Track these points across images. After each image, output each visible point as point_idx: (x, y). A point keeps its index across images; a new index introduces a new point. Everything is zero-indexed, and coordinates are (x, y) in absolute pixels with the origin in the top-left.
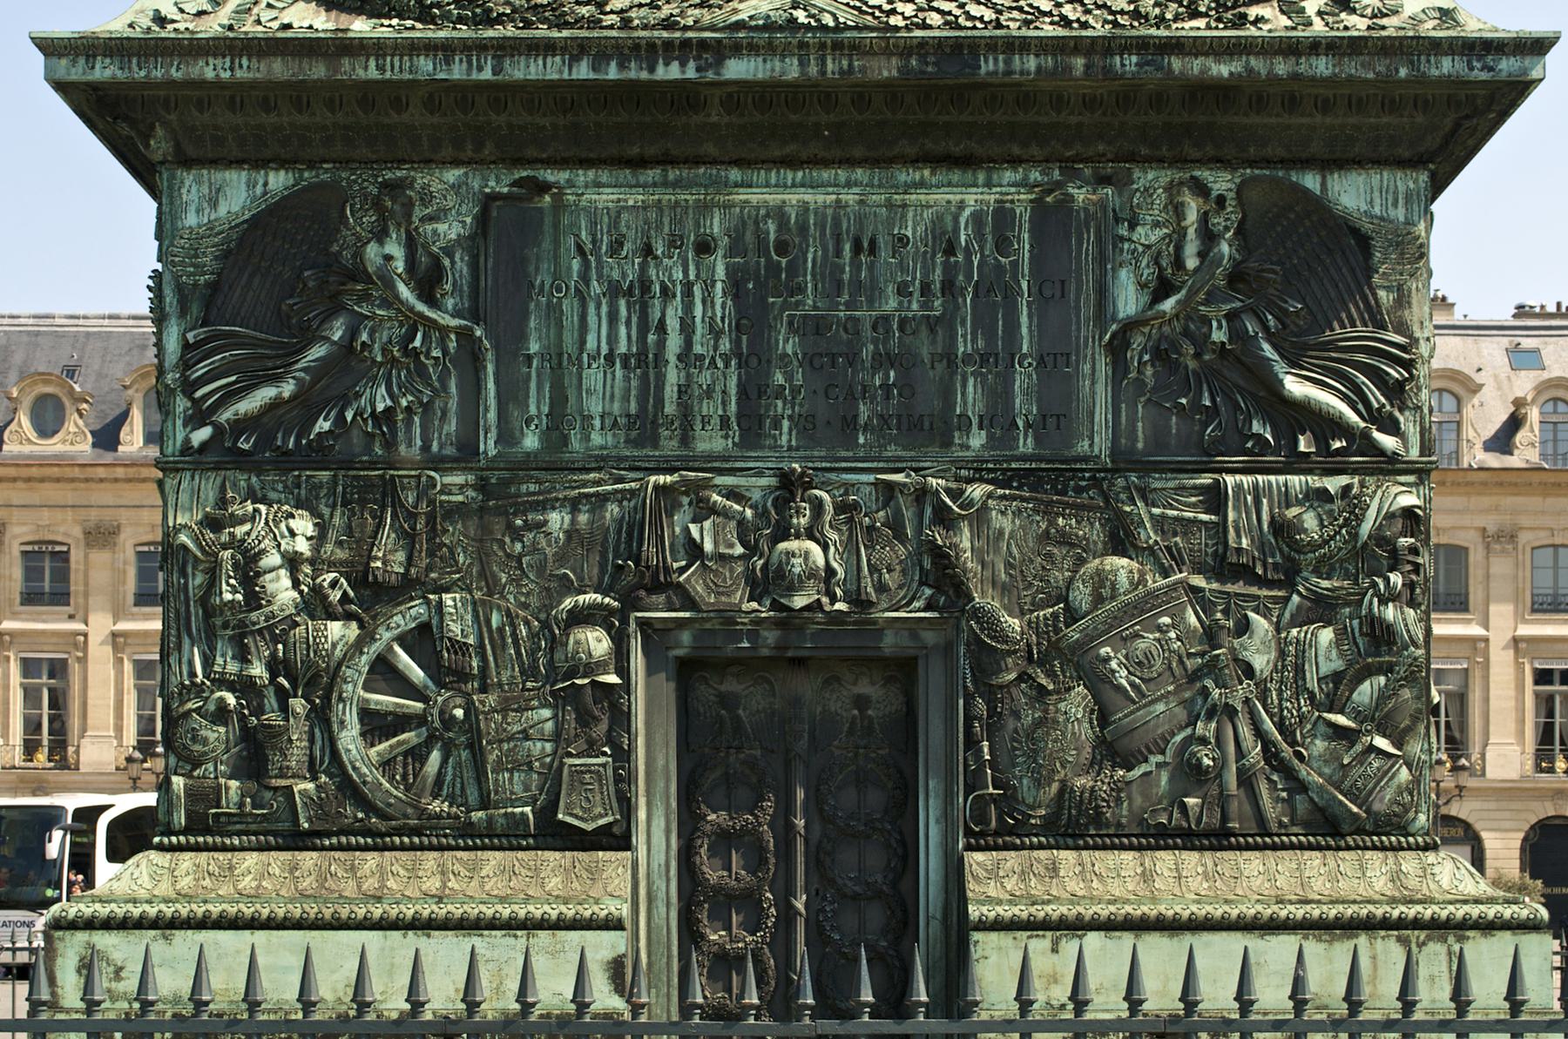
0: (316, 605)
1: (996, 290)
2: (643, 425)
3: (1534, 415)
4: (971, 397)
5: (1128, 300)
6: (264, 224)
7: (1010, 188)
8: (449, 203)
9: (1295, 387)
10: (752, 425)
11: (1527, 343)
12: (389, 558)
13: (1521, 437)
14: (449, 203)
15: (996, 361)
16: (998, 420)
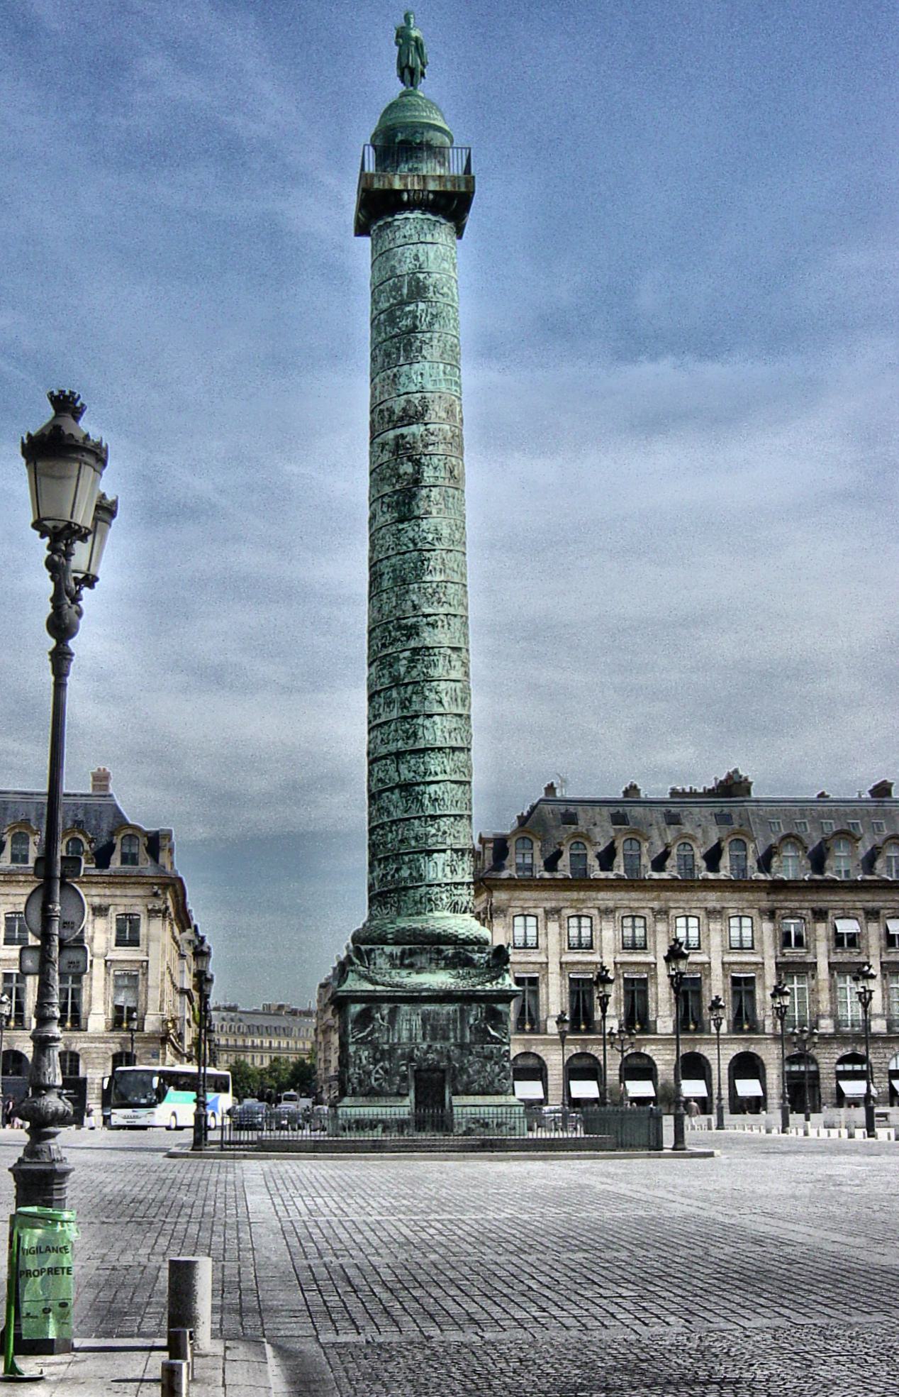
0: (369, 1063)
1: (455, 1021)
2: (410, 1038)
3: (674, 851)
4: (452, 1034)
5: (472, 1021)
6: (363, 1011)
7: (456, 1006)
8: (386, 1009)
9: (493, 1033)
10: (424, 1038)
11: (673, 810)
12: (378, 1056)
13: (668, 863)
14: (386, 1009)
15: (455, 1030)
16: (455, 1038)
